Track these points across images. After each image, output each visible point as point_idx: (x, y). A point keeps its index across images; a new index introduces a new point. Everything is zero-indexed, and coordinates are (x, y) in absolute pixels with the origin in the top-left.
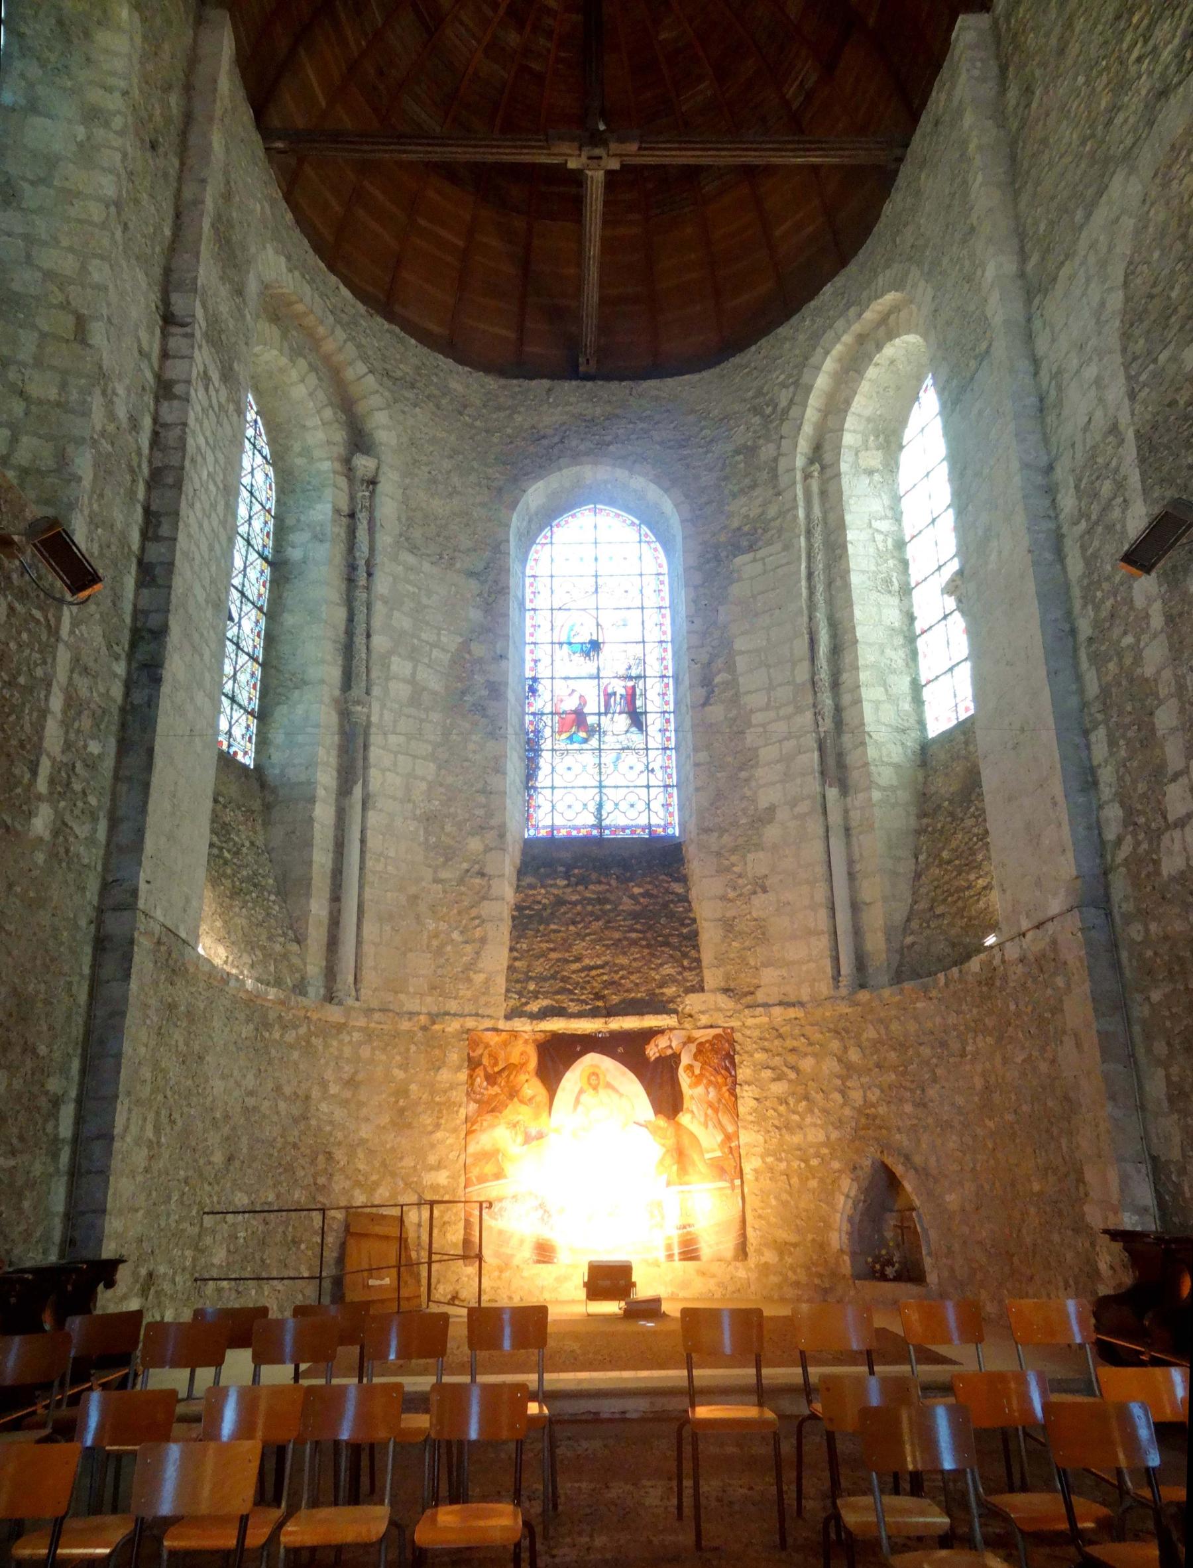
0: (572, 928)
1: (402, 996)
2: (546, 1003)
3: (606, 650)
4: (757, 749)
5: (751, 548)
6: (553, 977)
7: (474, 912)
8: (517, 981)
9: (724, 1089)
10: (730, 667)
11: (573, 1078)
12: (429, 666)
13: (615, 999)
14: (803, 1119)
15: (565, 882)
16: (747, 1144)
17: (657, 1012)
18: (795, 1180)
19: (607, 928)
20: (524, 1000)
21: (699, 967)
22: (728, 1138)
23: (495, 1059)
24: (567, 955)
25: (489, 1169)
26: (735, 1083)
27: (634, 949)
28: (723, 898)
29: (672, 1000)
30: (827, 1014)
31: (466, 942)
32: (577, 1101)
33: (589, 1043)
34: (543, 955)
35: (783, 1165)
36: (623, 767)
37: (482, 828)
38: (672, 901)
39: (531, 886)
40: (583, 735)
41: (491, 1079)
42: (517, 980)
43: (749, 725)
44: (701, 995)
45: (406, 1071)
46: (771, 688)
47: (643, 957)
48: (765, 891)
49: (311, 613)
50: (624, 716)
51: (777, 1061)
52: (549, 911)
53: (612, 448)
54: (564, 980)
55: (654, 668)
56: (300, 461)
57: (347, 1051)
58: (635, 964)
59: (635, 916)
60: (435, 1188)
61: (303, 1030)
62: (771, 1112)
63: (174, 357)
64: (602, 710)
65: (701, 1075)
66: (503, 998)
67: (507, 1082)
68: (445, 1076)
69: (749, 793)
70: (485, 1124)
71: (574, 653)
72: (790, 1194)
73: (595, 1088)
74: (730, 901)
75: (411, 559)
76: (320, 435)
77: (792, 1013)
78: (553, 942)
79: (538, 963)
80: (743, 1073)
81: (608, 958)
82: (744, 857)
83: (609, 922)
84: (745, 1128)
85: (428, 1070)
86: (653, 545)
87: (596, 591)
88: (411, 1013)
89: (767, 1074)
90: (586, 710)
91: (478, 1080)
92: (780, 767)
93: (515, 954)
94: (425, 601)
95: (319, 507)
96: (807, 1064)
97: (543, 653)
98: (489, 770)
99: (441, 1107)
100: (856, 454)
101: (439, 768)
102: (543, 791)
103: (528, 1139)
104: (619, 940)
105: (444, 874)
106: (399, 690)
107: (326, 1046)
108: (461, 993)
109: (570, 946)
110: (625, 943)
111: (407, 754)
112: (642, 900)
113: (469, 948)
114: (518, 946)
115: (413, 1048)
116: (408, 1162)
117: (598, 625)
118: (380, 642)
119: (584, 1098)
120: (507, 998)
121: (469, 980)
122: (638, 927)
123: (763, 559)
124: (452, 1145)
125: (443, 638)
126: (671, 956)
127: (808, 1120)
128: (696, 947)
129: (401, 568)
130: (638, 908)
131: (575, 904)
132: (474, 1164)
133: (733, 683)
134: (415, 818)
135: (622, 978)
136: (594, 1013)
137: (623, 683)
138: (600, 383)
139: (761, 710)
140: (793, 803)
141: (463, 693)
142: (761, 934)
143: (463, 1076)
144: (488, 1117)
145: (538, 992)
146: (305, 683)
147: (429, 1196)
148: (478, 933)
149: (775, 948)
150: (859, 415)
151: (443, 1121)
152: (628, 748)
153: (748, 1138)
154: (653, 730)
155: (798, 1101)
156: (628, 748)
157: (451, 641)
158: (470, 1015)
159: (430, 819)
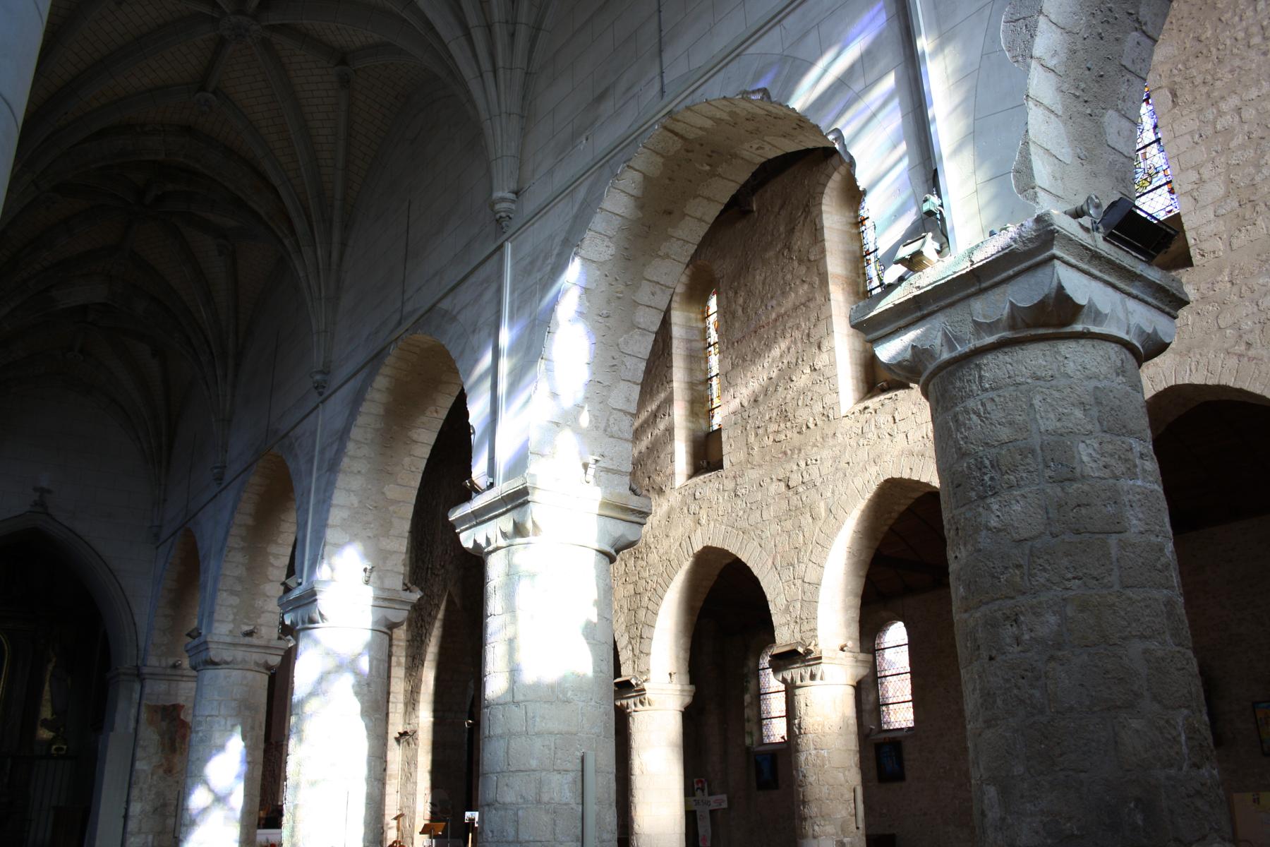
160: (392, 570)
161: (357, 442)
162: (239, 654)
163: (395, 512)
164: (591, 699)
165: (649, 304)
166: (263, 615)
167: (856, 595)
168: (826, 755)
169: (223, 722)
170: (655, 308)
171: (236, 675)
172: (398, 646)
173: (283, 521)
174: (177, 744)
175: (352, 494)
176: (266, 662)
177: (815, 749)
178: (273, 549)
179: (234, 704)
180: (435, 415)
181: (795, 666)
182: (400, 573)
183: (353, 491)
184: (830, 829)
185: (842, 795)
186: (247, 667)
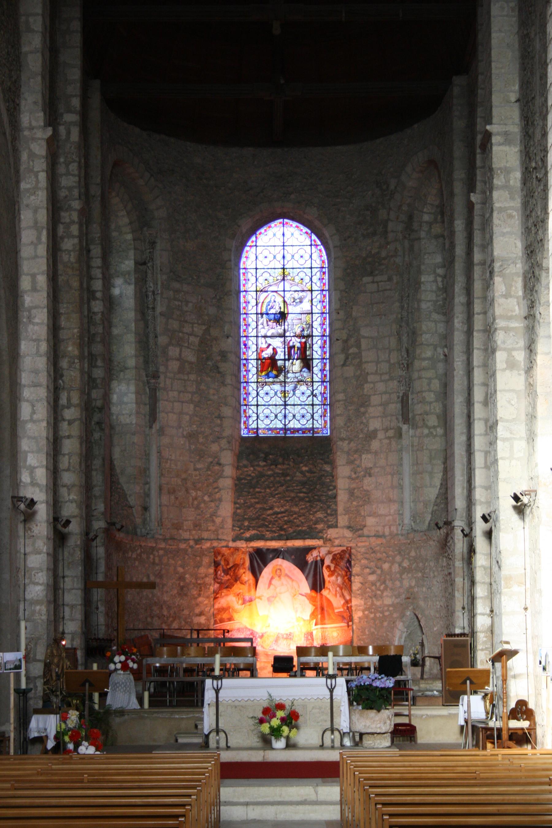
0: (268, 490)
1: (181, 531)
2: (254, 532)
3: (290, 317)
4: (370, 396)
5: (371, 274)
6: (258, 518)
7: (215, 485)
8: (238, 521)
9: (346, 578)
10: (359, 346)
11: (267, 572)
12: (188, 348)
13: (291, 530)
14: (382, 593)
15: (264, 463)
16: (356, 605)
17: (312, 538)
18: (377, 622)
19: (287, 491)
20: (242, 531)
21: (336, 514)
22: (347, 602)
23: (227, 562)
24: (265, 506)
25: (225, 616)
26: (351, 575)
27: (301, 503)
28: (350, 478)
29: (321, 531)
30: (396, 542)
31: (212, 501)
32: (270, 583)
33: (277, 553)
34: (252, 505)
35: (372, 616)
36: (298, 392)
37: (219, 438)
38: (324, 475)
39: (245, 466)
40: (275, 372)
41: (226, 572)
43: (367, 382)
44: (336, 529)
45: (184, 568)
46: (378, 362)
47: (306, 508)
48: (370, 475)
49: (127, 327)
50: (299, 361)
51: (372, 564)
52: (255, 480)
53: (293, 196)
54: (264, 519)
56: (114, 234)
57: (157, 560)
58: (301, 511)
59: (304, 484)
60: (199, 624)
61: (139, 551)
62: (368, 589)
63: (95, 279)
64: (287, 357)
65: (334, 571)
66: (231, 530)
67: (234, 573)
68: (202, 570)
69: (365, 421)
70: (223, 594)
71: (270, 320)
72: (375, 629)
73: (279, 577)
74: (353, 479)
75: (176, 285)
76: (126, 220)
77: (379, 541)
78: (258, 498)
79: (250, 510)
80: (356, 569)
82: (361, 456)
83: (288, 487)
84: (355, 597)
85: (194, 567)
86: (319, 247)
87: (284, 279)
88: (185, 540)
89: (368, 570)
90: (277, 357)
91: (219, 572)
92: (380, 408)
93: (238, 506)
94: (185, 308)
95: (127, 262)
97: (252, 319)
98: (221, 404)
99: (201, 587)
100: (430, 226)
101: (195, 406)
102: (252, 407)
103: (244, 602)
104: (294, 498)
105: (199, 466)
106: (174, 365)
107: (148, 558)
108: (209, 528)
109: (267, 500)
110: (297, 499)
111: (179, 401)
112: (307, 474)
113: (213, 504)
114: (239, 501)
115: (187, 557)
116: (186, 612)
117: (284, 302)
118: (163, 340)
119: (274, 582)
120: (233, 530)
121: (213, 521)
122: (304, 490)
123: (377, 282)
124: (206, 604)
125: (195, 329)
126: (321, 507)
127: (385, 594)
128: (336, 503)
129: (171, 293)
130: (305, 479)
131: (269, 476)
132: (218, 614)
133: (358, 355)
134: (183, 436)
135: (295, 518)
136: (279, 538)
137: (299, 340)
138: (286, 149)
139: (372, 374)
140: (386, 430)
141: (208, 359)
142: (367, 498)
143: (211, 570)
144: (225, 591)
145: (250, 527)
146: (126, 368)
147: (196, 628)
148: (217, 496)
149: (374, 507)
150: (432, 205)
151: (202, 593)
152: (301, 381)
153: (355, 602)
154: (316, 370)
155: (381, 585)
156: (301, 381)
157: (199, 330)
158: (214, 540)
159: (191, 436)
172: (507, 330)
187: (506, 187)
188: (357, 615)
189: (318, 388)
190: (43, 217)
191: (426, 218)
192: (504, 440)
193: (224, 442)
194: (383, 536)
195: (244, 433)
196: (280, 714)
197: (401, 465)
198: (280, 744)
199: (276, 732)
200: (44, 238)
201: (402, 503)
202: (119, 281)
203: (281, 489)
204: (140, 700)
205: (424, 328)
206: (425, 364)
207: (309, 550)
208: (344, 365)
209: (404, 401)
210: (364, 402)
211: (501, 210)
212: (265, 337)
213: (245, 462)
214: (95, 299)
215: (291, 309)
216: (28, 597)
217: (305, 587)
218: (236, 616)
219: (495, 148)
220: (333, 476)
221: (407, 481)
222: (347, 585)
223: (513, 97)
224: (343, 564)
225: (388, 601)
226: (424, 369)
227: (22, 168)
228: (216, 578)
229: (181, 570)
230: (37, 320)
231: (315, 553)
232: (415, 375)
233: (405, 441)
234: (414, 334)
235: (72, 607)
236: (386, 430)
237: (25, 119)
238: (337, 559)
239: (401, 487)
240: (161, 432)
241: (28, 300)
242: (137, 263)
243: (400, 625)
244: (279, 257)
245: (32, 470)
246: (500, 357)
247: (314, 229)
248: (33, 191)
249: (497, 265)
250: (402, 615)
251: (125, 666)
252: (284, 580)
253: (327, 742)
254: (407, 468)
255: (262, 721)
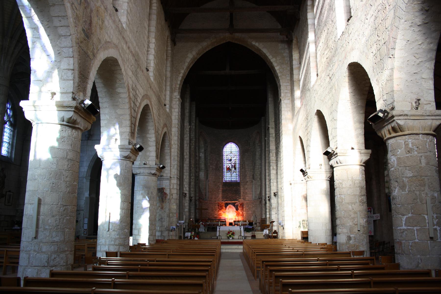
2: (225, 200)
3: (232, 160)
11: (228, 207)
22: (243, 213)
23: (220, 205)
25: (220, 215)
28: (243, 190)
33: (230, 204)
41: (220, 207)
42: (223, 197)
55: (237, 163)
56: (200, 145)
68: (216, 207)
77: (248, 201)
81: (232, 195)
96: (250, 206)
97: (225, 160)
99: (216, 210)
103: (224, 212)
105: (216, 187)
106: (211, 169)
116: (213, 214)
118: (209, 164)
136: (230, 201)
140: (250, 181)
143: (218, 207)
153: (244, 213)
159: (214, 182)
160: (124, 138)
161: (101, 97)
162: (142, 171)
163: (122, 118)
164: (45, 178)
165: (61, 25)
166: (150, 158)
167: (360, 123)
168: (343, 197)
169: (139, 192)
170: (65, 26)
171: (142, 177)
172: (273, 163)
173: (148, 126)
174: (164, 200)
175: (106, 115)
176: (151, 172)
177: (339, 195)
178: (148, 136)
179: (141, 187)
180: (120, 82)
181: (332, 158)
182: (127, 139)
183: (107, 114)
184: (345, 231)
185: (350, 216)
186: (145, 175)
187: (272, 137)
188: (244, 215)
189: (237, 173)
190: (188, 142)
191: (257, 142)
192: (272, 183)
193: (220, 183)
194: (249, 200)
195: (224, 181)
196: (231, 233)
197: (252, 187)
198: (231, 238)
199: (230, 236)
200: (188, 146)
201: (253, 194)
202: (201, 154)
203: (231, 192)
204: (205, 230)
205: (257, 162)
206: (257, 169)
207: (236, 203)
208: (242, 169)
209: (253, 175)
210: (246, 176)
211: (271, 141)
212: (228, 164)
213: (224, 187)
214: (197, 157)
215: (232, 159)
216: (185, 211)
217: (235, 210)
218: (222, 215)
219: (270, 130)
220: (240, 189)
221: (254, 190)
222: (243, 209)
223: (273, 121)
224: (242, 205)
225: (250, 212)
226: (257, 170)
227: (185, 133)
228: (218, 208)
229: (212, 206)
230: (187, 161)
231: (237, 204)
232: (255, 171)
233: (253, 183)
234: (255, 163)
235: (193, 213)
236: (250, 181)
237: (185, 124)
238: (241, 205)
239: (253, 191)
240: (209, 181)
241: (185, 157)
242: (204, 150)
243: (252, 217)
244: (230, 149)
245: (186, 188)
246: (271, 167)
247: (236, 144)
248: (187, 137)
249: (271, 151)
250: (253, 215)
251: (202, 224)
252: (231, 208)
253: (240, 238)
254: (254, 188)
255: (228, 234)
